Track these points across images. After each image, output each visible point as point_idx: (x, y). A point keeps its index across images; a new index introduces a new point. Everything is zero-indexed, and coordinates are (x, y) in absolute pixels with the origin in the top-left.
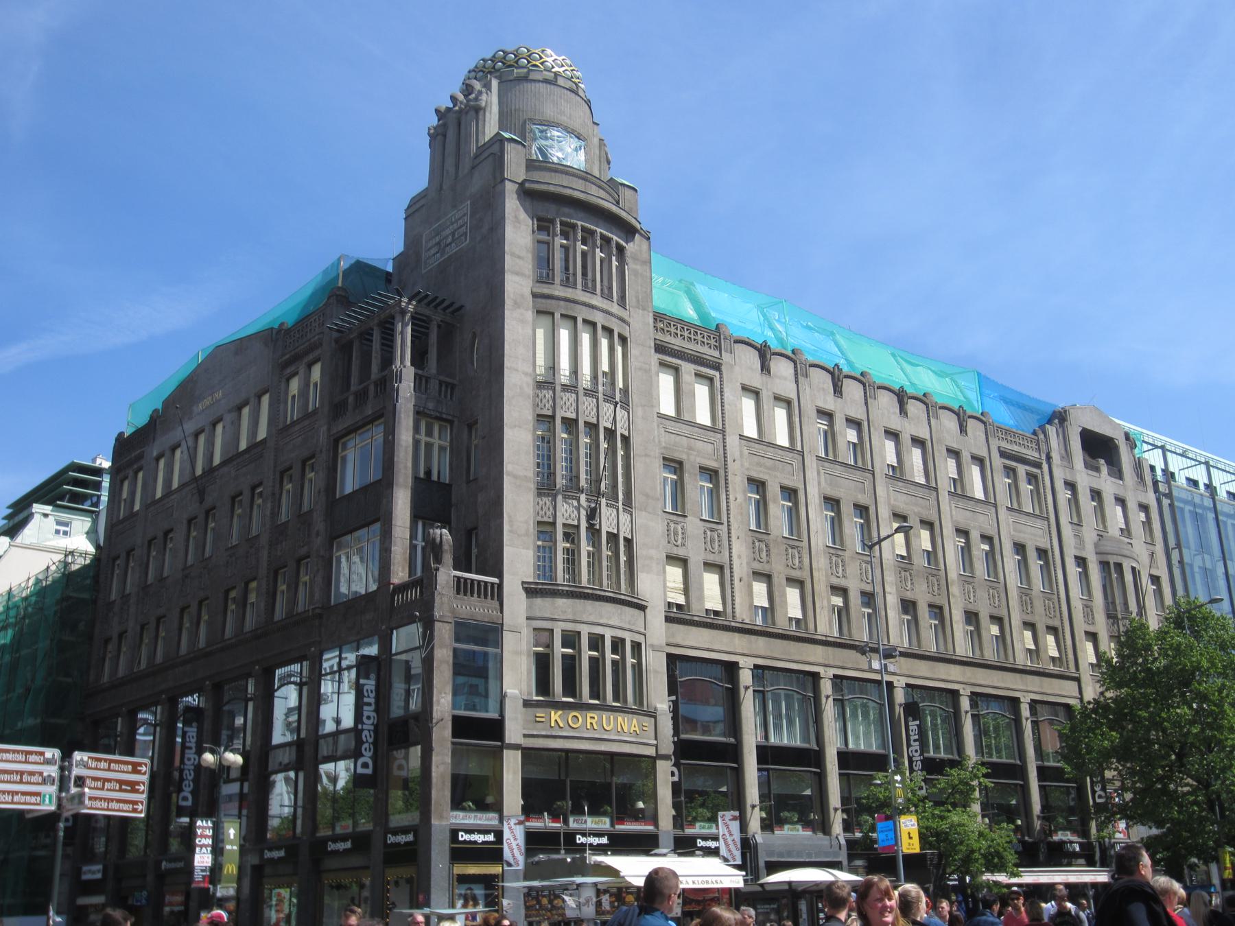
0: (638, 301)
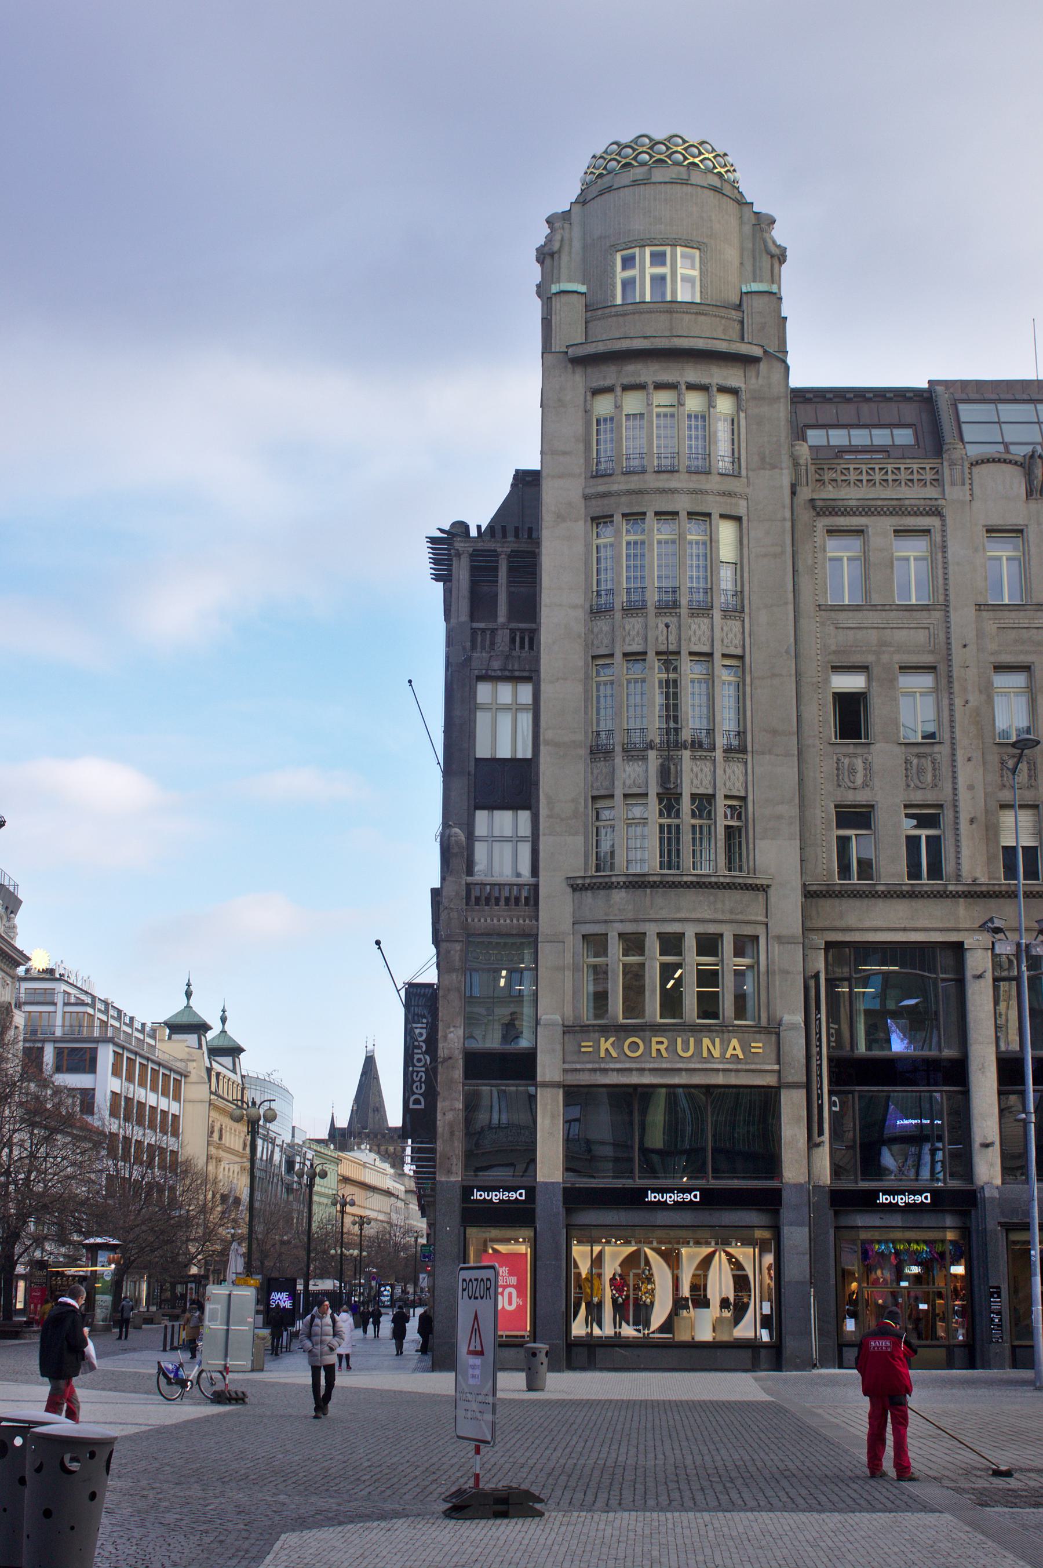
0: (763, 459)
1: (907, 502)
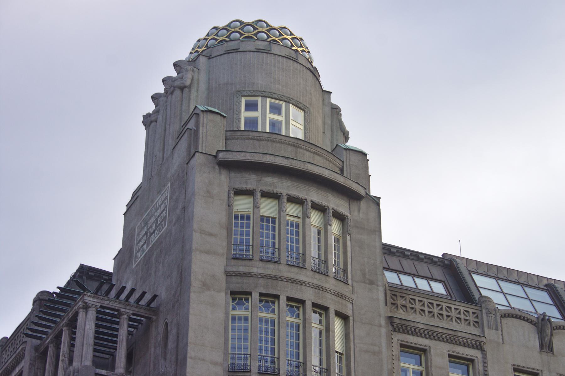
0: (364, 275)
1: (460, 334)
